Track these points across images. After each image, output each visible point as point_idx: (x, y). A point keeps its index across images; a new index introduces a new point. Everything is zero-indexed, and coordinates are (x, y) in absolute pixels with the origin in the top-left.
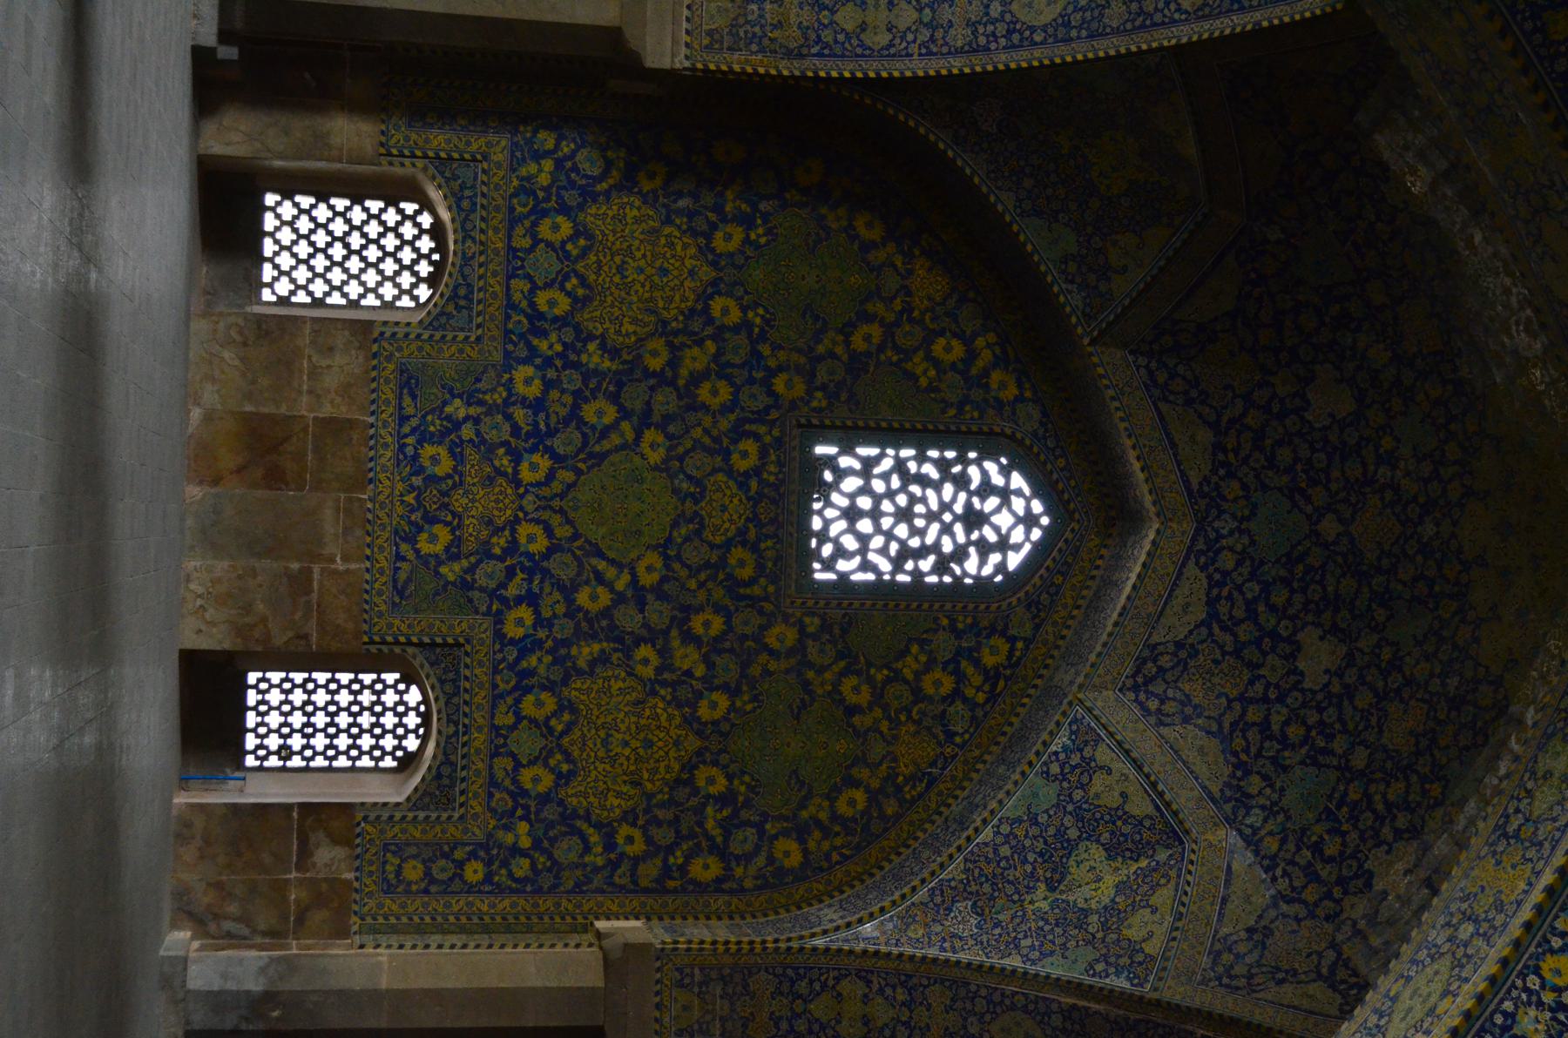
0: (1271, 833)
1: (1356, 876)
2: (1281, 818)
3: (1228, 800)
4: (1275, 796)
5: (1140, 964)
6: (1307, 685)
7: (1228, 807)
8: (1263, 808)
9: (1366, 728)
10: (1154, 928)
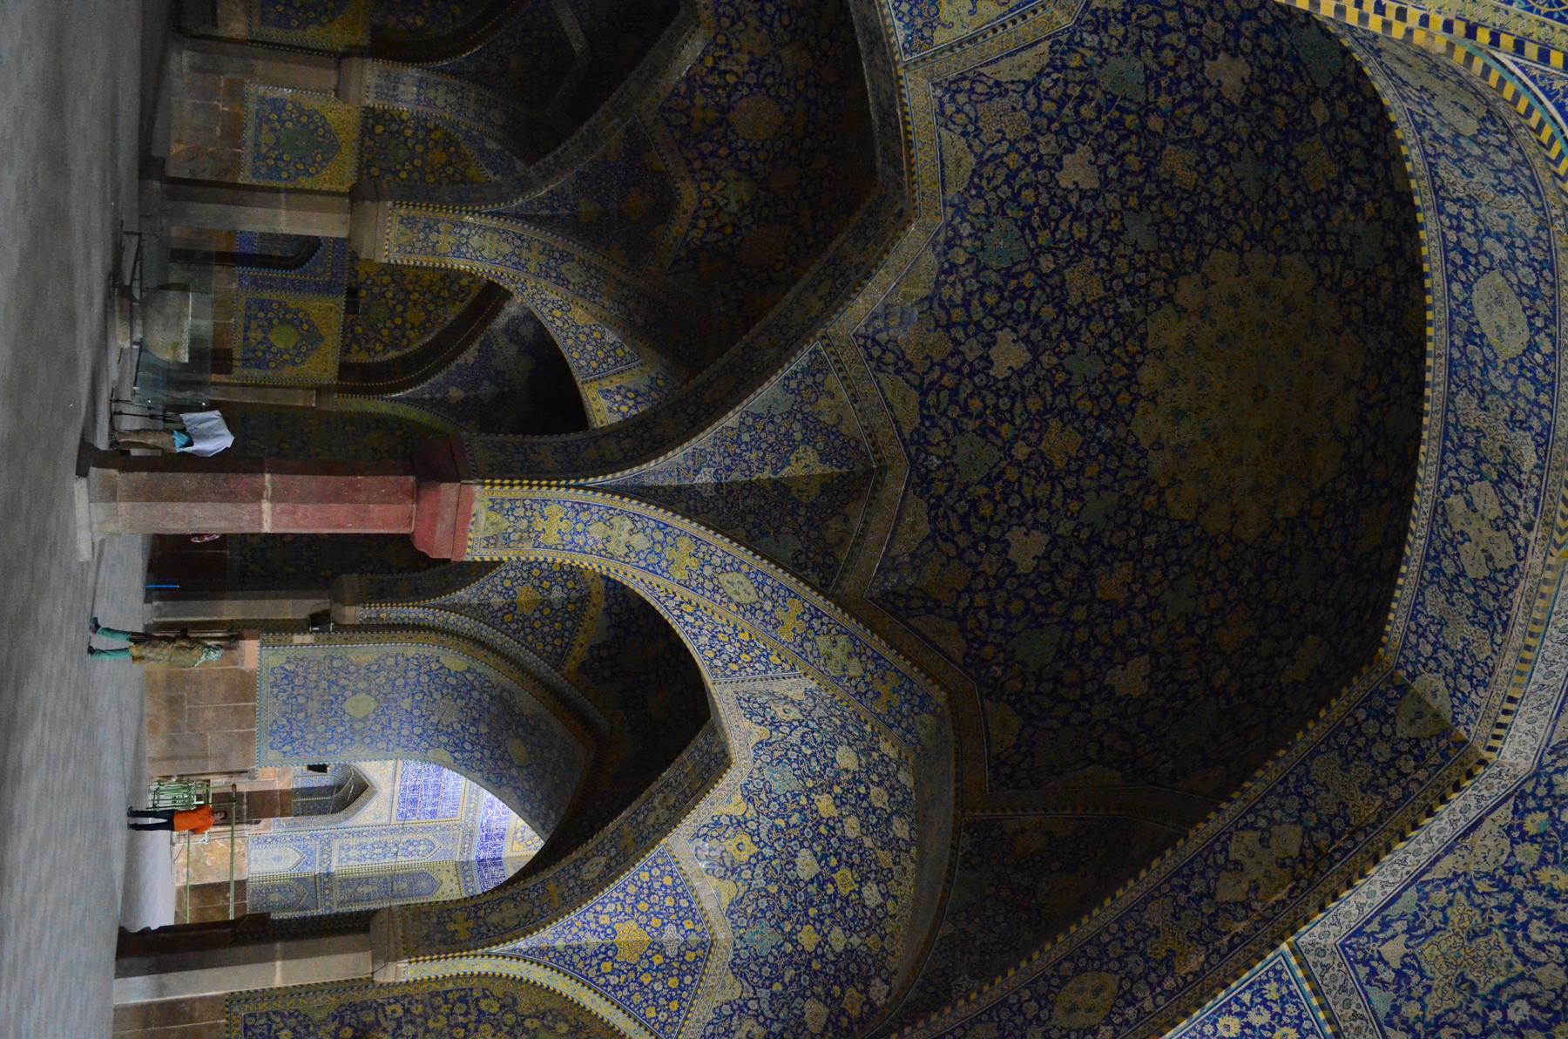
0: (1083, 56)
1: (1070, 139)
2: (1099, 60)
3: (1093, 13)
4: (1114, 50)
5: (922, 38)
6: (1207, 63)
7: (1088, 16)
8: (1101, 43)
9: (1177, 128)
10: (958, 24)
